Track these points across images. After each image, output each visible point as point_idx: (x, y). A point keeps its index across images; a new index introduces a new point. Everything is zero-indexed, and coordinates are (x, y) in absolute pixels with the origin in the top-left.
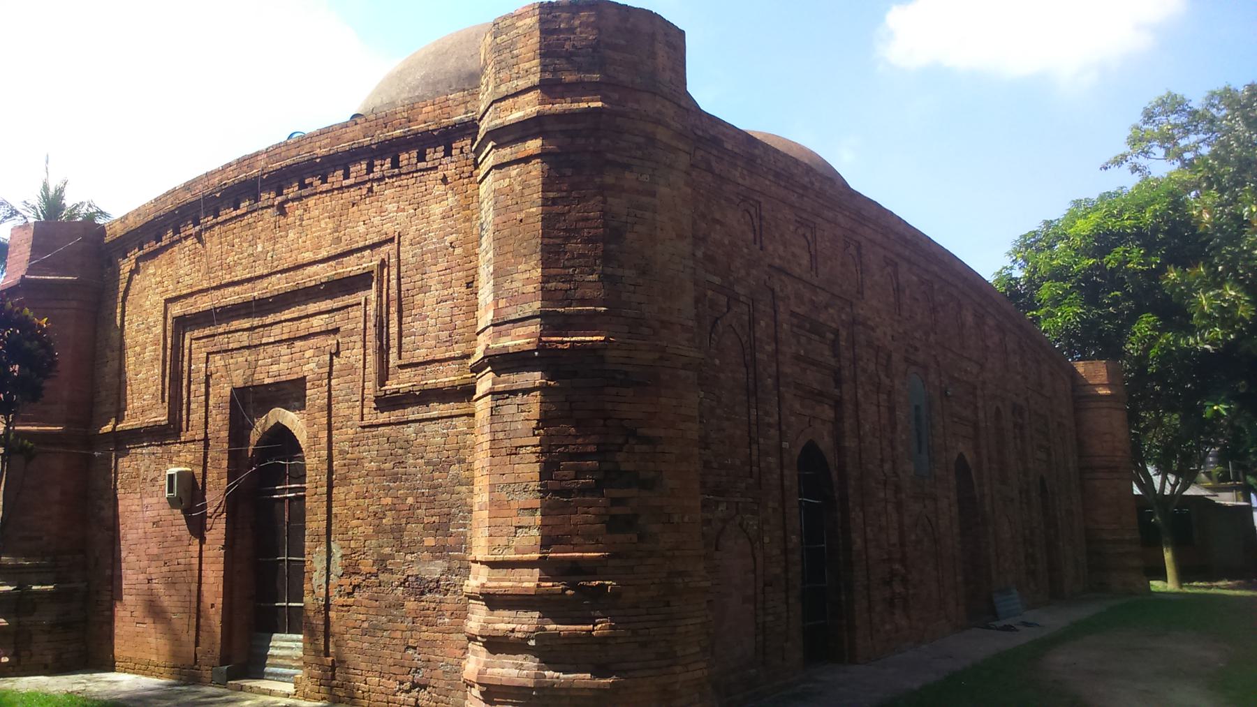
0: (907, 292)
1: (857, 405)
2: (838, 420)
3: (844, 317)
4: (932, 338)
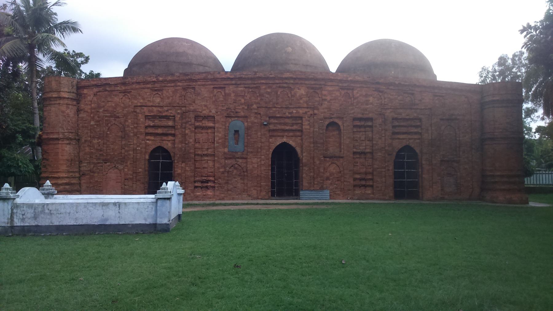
0: (233, 95)
1: (184, 135)
2: (174, 140)
3: (179, 111)
4: (255, 106)
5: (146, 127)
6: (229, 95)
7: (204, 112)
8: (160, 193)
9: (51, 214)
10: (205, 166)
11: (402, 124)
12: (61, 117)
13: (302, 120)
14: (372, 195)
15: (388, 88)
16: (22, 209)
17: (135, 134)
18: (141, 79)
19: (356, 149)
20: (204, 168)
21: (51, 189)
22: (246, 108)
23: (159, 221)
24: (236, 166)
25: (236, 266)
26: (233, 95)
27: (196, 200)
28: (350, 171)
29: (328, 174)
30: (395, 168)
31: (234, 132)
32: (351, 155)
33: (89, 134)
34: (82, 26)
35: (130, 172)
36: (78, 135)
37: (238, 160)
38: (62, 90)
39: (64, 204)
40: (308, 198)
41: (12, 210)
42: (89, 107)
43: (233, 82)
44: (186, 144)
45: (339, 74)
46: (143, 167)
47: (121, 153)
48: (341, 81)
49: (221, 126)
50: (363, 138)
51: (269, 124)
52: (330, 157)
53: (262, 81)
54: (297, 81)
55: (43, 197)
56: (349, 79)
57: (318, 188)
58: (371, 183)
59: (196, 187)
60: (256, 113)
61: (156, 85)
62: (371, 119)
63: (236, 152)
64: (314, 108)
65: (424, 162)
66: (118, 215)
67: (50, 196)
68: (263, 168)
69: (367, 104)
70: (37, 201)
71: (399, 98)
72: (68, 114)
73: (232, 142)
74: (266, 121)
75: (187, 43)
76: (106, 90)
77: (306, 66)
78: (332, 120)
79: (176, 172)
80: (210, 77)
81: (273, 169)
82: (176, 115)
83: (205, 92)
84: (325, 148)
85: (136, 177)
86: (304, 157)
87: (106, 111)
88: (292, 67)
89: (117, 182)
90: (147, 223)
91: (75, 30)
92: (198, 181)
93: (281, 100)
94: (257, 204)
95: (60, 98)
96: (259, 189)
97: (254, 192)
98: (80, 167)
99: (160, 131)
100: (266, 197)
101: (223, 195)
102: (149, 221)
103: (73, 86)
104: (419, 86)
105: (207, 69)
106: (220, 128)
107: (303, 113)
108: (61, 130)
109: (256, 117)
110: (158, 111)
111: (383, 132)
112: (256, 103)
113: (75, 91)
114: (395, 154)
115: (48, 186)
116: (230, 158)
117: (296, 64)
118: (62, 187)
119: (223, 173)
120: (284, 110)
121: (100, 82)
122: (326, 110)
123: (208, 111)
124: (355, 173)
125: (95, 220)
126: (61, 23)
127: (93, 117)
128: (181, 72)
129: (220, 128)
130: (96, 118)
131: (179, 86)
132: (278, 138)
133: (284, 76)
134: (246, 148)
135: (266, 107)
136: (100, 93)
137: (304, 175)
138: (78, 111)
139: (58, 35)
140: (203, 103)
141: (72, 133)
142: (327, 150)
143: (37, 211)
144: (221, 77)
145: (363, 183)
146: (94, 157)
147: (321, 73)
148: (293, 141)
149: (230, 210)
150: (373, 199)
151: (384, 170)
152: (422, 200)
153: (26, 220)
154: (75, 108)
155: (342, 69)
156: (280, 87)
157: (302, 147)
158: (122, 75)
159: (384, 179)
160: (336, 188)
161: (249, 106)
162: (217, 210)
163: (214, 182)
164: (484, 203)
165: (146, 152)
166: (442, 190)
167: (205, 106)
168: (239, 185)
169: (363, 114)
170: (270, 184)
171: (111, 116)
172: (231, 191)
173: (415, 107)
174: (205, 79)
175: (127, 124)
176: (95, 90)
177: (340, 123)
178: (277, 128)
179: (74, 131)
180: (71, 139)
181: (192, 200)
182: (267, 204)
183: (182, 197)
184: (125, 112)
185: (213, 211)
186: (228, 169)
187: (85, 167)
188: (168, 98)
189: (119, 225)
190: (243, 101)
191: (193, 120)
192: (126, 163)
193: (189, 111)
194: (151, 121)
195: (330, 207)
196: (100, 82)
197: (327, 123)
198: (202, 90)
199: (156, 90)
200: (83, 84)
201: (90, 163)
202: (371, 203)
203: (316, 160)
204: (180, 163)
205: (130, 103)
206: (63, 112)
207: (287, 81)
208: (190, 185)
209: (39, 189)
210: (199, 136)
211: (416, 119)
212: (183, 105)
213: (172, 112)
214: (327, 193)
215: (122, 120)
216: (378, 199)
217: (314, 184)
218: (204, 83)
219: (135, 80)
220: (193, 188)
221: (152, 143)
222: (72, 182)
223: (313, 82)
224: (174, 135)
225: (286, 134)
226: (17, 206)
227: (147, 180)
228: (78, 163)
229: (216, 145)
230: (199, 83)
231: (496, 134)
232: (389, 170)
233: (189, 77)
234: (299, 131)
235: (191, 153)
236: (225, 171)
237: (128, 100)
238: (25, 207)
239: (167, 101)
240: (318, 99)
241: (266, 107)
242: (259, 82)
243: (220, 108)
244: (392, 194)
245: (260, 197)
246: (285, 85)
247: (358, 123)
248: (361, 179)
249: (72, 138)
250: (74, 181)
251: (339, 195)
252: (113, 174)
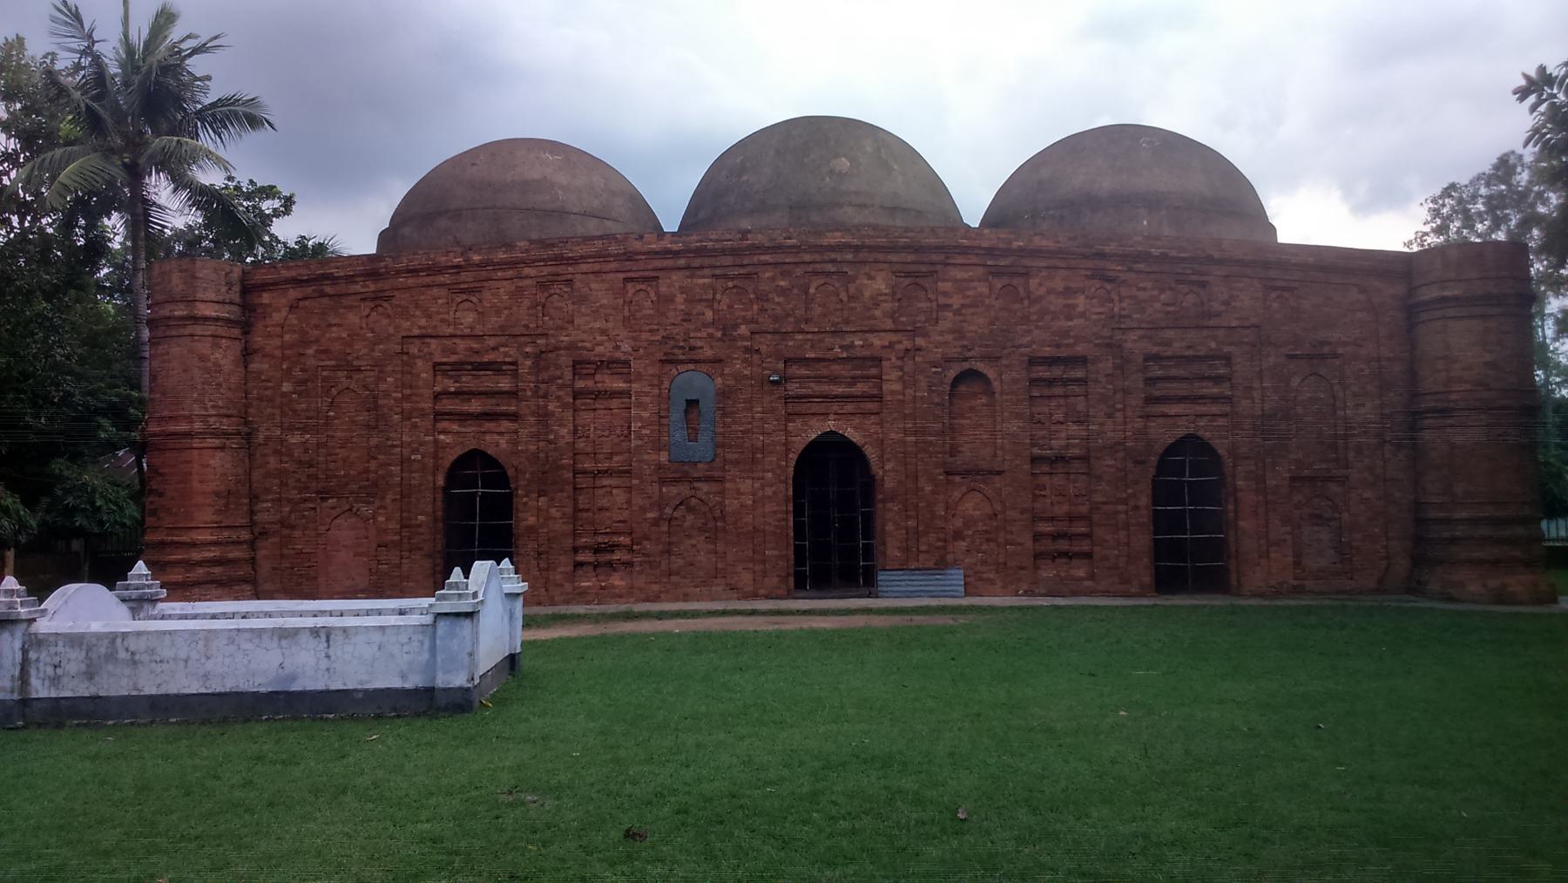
0: (680, 298)
1: (543, 417)
2: (516, 432)
4: (743, 330)
5: (437, 397)
6: (670, 299)
7: (599, 349)
8: (444, 597)
9: (135, 663)
10: (604, 502)
11: (1174, 372)
12: (194, 376)
13: (880, 366)
14: (1087, 583)
15: (1130, 270)
16: (53, 650)
17: (406, 416)
18: (420, 260)
19: (1041, 447)
21: (149, 586)
22: (719, 334)
23: (442, 681)
24: (694, 501)
25: (629, 835)
26: (680, 298)
27: (579, 603)
28: (1023, 512)
29: (959, 523)
30: (1155, 503)
31: (683, 407)
32: (1027, 467)
33: (278, 418)
34: (273, 111)
35: (393, 525)
36: (246, 423)
38: (200, 296)
39: (170, 633)
40: (901, 595)
41: (25, 652)
42: (277, 342)
43: (682, 262)
44: (550, 442)
45: (986, 231)
46: (429, 509)
47: (367, 471)
48: (990, 251)
49: (647, 389)
50: (1059, 416)
51: (785, 379)
52: (966, 473)
53: (767, 258)
54: (862, 255)
55: (123, 609)
56: (1016, 244)
57: (931, 564)
58: (1084, 546)
59: (578, 565)
60: (747, 350)
61: (464, 276)
62: (1082, 361)
63: (695, 464)
64: (914, 332)
65: (1240, 483)
66: (324, 664)
67: (146, 606)
68: (769, 508)
69: (1071, 319)
70: (96, 627)
71: (1162, 297)
72: (216, 364)
73: (679, 435)
74: (776, 372)
75: (551, 153)
76: (323, 295)
77: (893, 210)
78: (966, 366)
80: (613, 249)
81: (798, 511)
82: (521, 360)
83: (600, 292)
84: (947, 447)
86: (887, 473)
87: (326, 351)
88: (850, 215)
89: (356, 555)
90: (408, 686)
91: (254, 122)
92: (585, 548)
93: (818, 310)
94: (753, 613)
95: (195, 319)
96: (758, 568)
97: (746, 578)
98: (252, 512)
99: (475, 406)
100: (780, 592)
101: (655, 587)
102: (414, 681)
103: (230, 285)
104: (1220, 262)
105: (612, 227)
106: (647, 394)
107: (884, 347)
108: (197, 410)
109: (745, 361)
110: (471, 349)
111: (1118, 396)
112: (746, 321)
113: (237, 299)
114: (1154, 459)
115: (140, 576)
116: (676, 481)
117: (862, 206)
118: (201, 571)
119: (656, 523)
120: (829, 340)
121: (305, 272)
122: (949, 337)
123: (610, 346)
124: (1036, 518)
125: (259, 681)
126: (213, 105)
127: (289, 370)
128: (534, 236)
129: (647, 394)
130: (297, 373)
131: (528, 277)
132: (814, 422)
133: (825, 242)
134: (719, 451)
135: (775, 332)
136: (307, 303)
137: (890, 527)
138: (247, 354)
139: (207, 140)
140: (597, 325)
141: (228, 416)
142: (954, 451)
143: (94, 656)
144: (646, 248)
145: (1063, 545)
146: (291, 482)
147: (933, 230)
148: (855, 428)
149: (668, 635)
150: (1091, 593)
151: (1121, 508)
152: (1238, 595)
153: (65, 680)
154: (237, 347)
155: (997, 215)
156: (815, 273)
157: (881, 443)
158: (371, 249)
159: (1123, 533)
160: (984, 563)
161: (727, 329)
162: (633, 635)
164: (1424, 604)
165: (436, 468)
166: (1297, 564)
167: (603, 332)
168: (701, 557)
169: (1058, 346)
170: (791, 552)
171: (337, 368)
172: (677, 573)
173: (1211, 323)
174: (602, 256)
175: (383, 387)
176: (294, 294)
177: (991, 374)
178: (809, 391)
179: (235, 412)
180: (226, 434)
181: (567, 602)
182: (779, 613)
183: (520, 602)
184: (377, 354)
185: (622, 637)
186: (668, 511)
187: (267, 513)
188: (498, 312)
189: (328, 692)
190: (709, 314)
191: (568, 374)
192: (383, 498)
193: (557, 349)
194: (451, 377)
195: (962, 620)
196: (305, 272)
197: (952, 374)
198: (593, 286)
199: (463, 291)
200: (259, 277)
201: (280, 500)
202: (1084, 607)
203: (922, 482)
204: (534, 495)
205: (391, 330)
206: (203, 358)
207: (838, 257)
208: (562, 559)
209: (111, 587)
210: (585, 417)
211: (1213, 358)
212: (540, 331)
213: (510, 352)
214: (956, 577)
215: (370, 376)
216: (1107, 593)
217: (919, 551)
218: (597, 267)
219: (403, 263)
220: (570, 568)
221: (454, 440)
222: (231, 555)
223: (910, 258)
224: (514, 417)
225: (835, 408)
226: (37, 642)
227: (439, 547)
228: (246, 501)
229: (634, 443)
230: (584, 267)
231: (1453, 397)
232: (1137, 508)
233: (556, 251)
234: (871, 397)
235: (562, 467)
236: (661, 518)
237: (385, 321)
238: (60, 644)
239: (494, 321)
240: (923, 305)
241: (775, 332)
242: (756, 258)
243: (644, 336)
244: (1148, 579)
245: (762, 592)
246: (830, 268)
247: (1042, 372)
248: (1055, 537)
249: (231, 429)
250: (235, 553)
251: (991, 582)
252: (344, 532)
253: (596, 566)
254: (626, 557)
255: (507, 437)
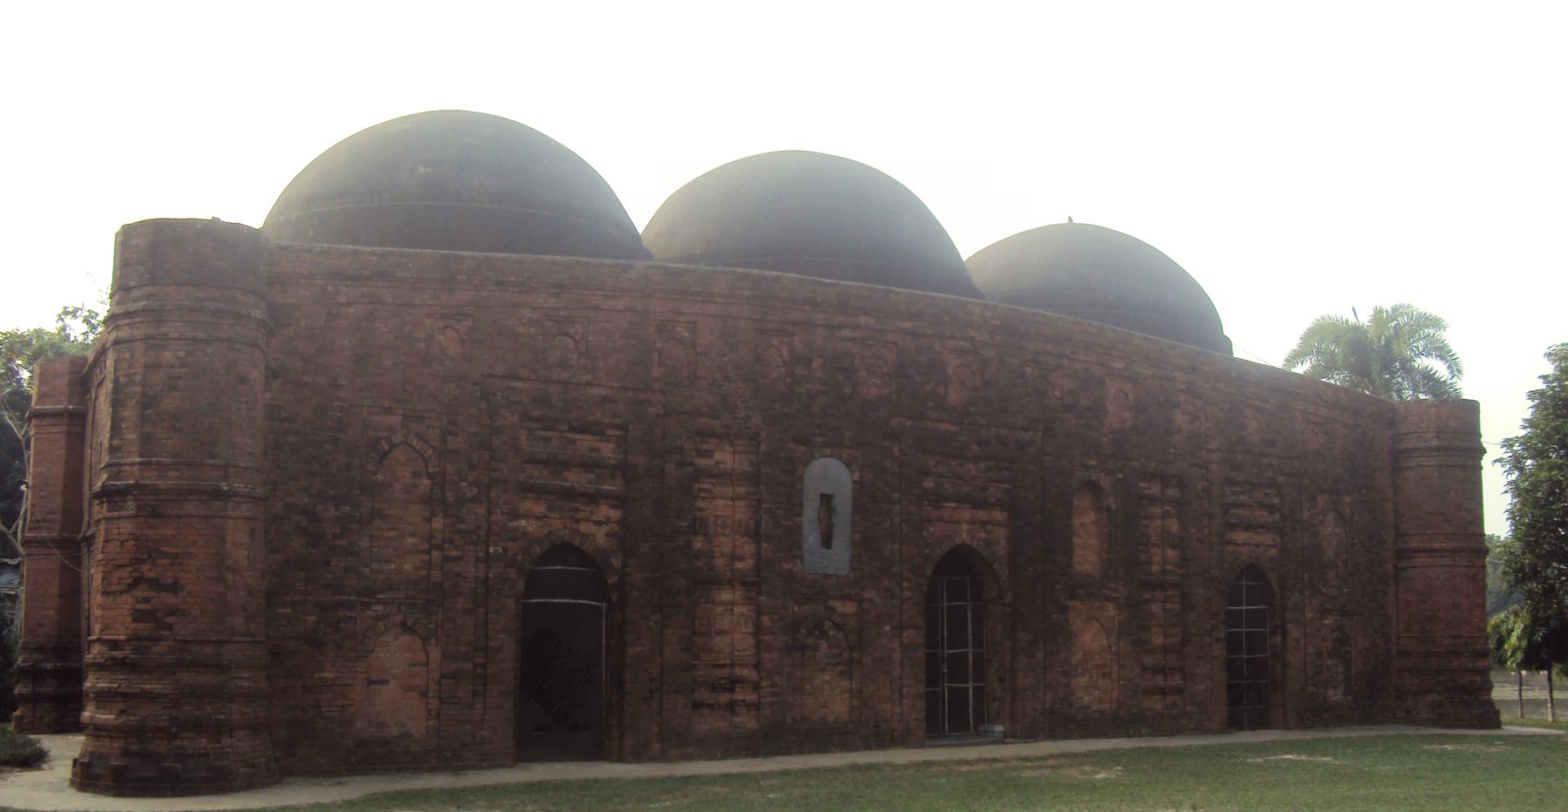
20: (721, 632)
37: (831, 603)
58: (1176, 681)
79: (631, 650)
85: (484, 666)
145: (1160, 680)
163: (756, 687)
171: (388, 411)
253: (711, 706)
254: (752, 697)
255: (605, 529)
